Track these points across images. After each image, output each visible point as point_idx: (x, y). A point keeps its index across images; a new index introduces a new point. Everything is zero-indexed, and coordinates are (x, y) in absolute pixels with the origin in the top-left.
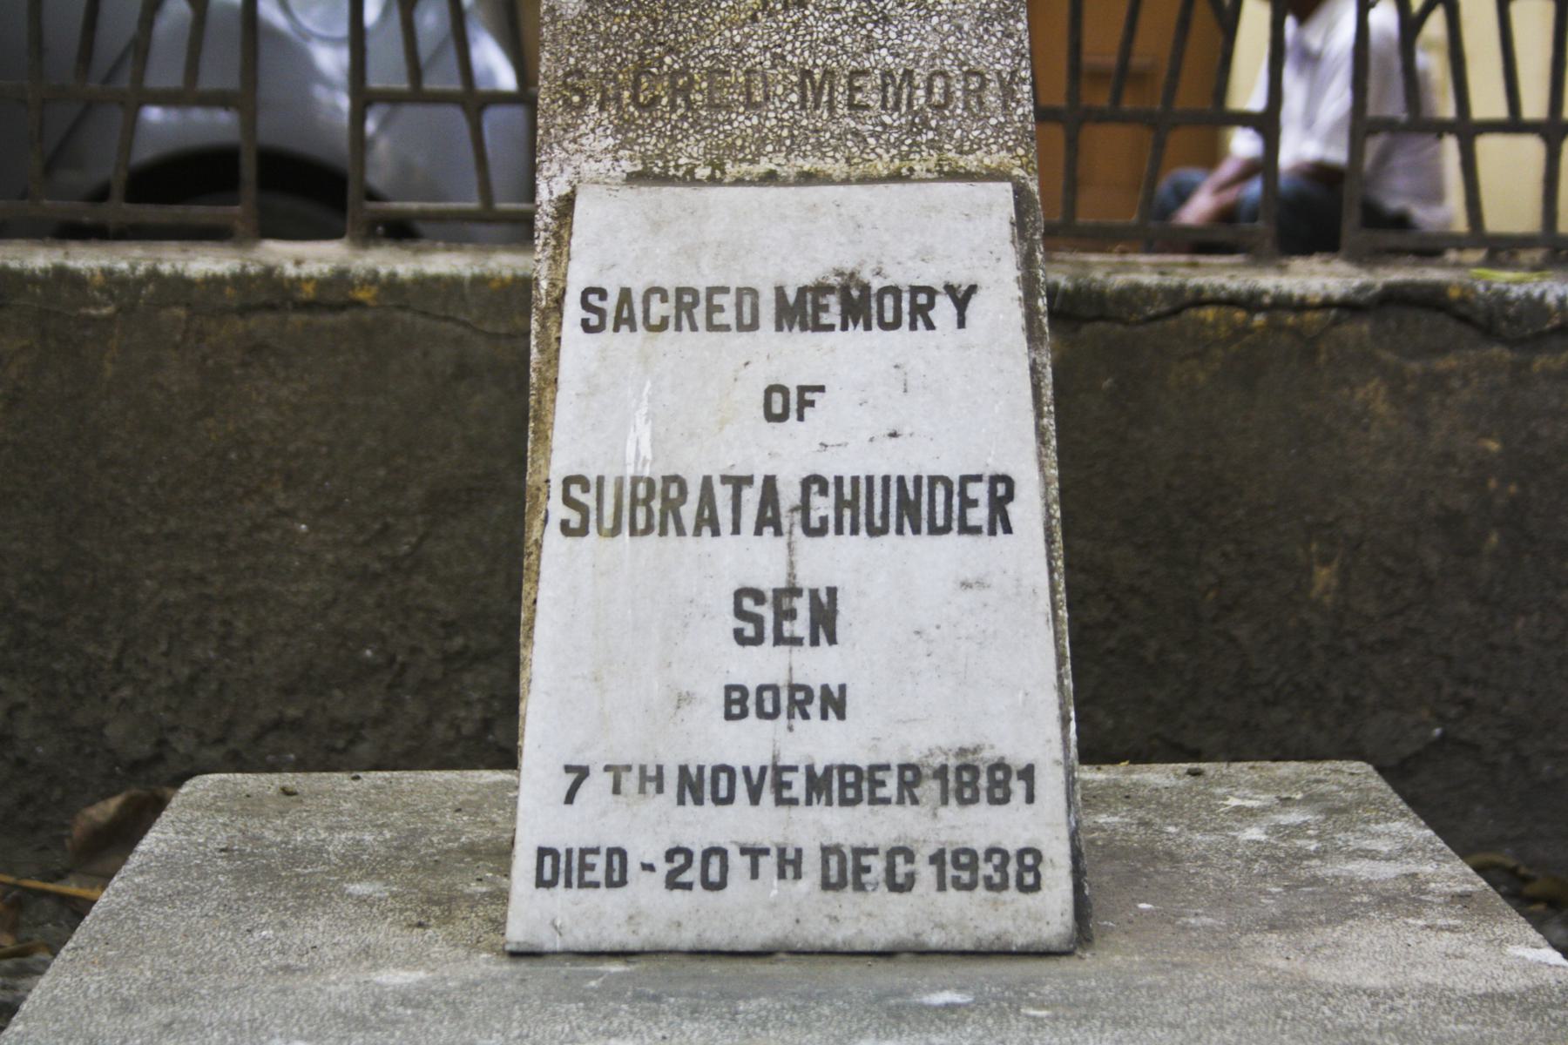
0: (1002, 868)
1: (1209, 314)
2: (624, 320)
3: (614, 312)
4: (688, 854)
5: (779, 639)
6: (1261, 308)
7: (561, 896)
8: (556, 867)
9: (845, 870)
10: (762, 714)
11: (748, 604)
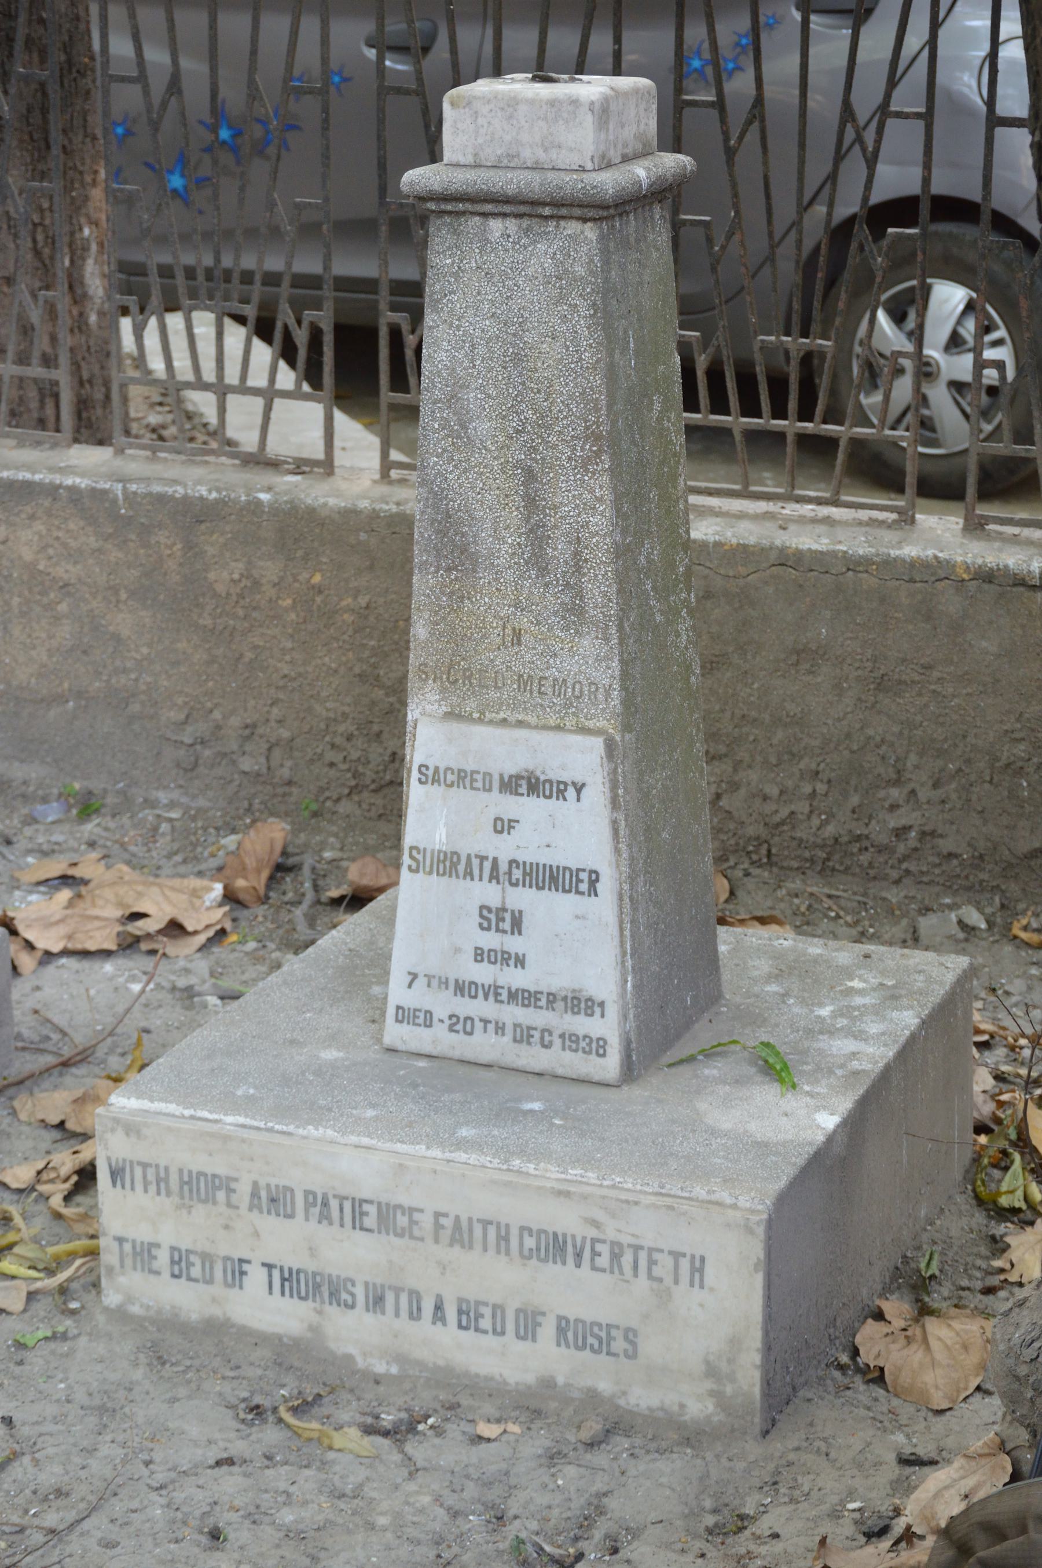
0: (590, 1044)
2: (435, 781)
3: (432, 776)
4: (458, 1018)
5: (498, 930)
7: (405, 1029)
8: (404, 1015)
9: (523, 1035)
10: (490, 962)
11: (485, 913)
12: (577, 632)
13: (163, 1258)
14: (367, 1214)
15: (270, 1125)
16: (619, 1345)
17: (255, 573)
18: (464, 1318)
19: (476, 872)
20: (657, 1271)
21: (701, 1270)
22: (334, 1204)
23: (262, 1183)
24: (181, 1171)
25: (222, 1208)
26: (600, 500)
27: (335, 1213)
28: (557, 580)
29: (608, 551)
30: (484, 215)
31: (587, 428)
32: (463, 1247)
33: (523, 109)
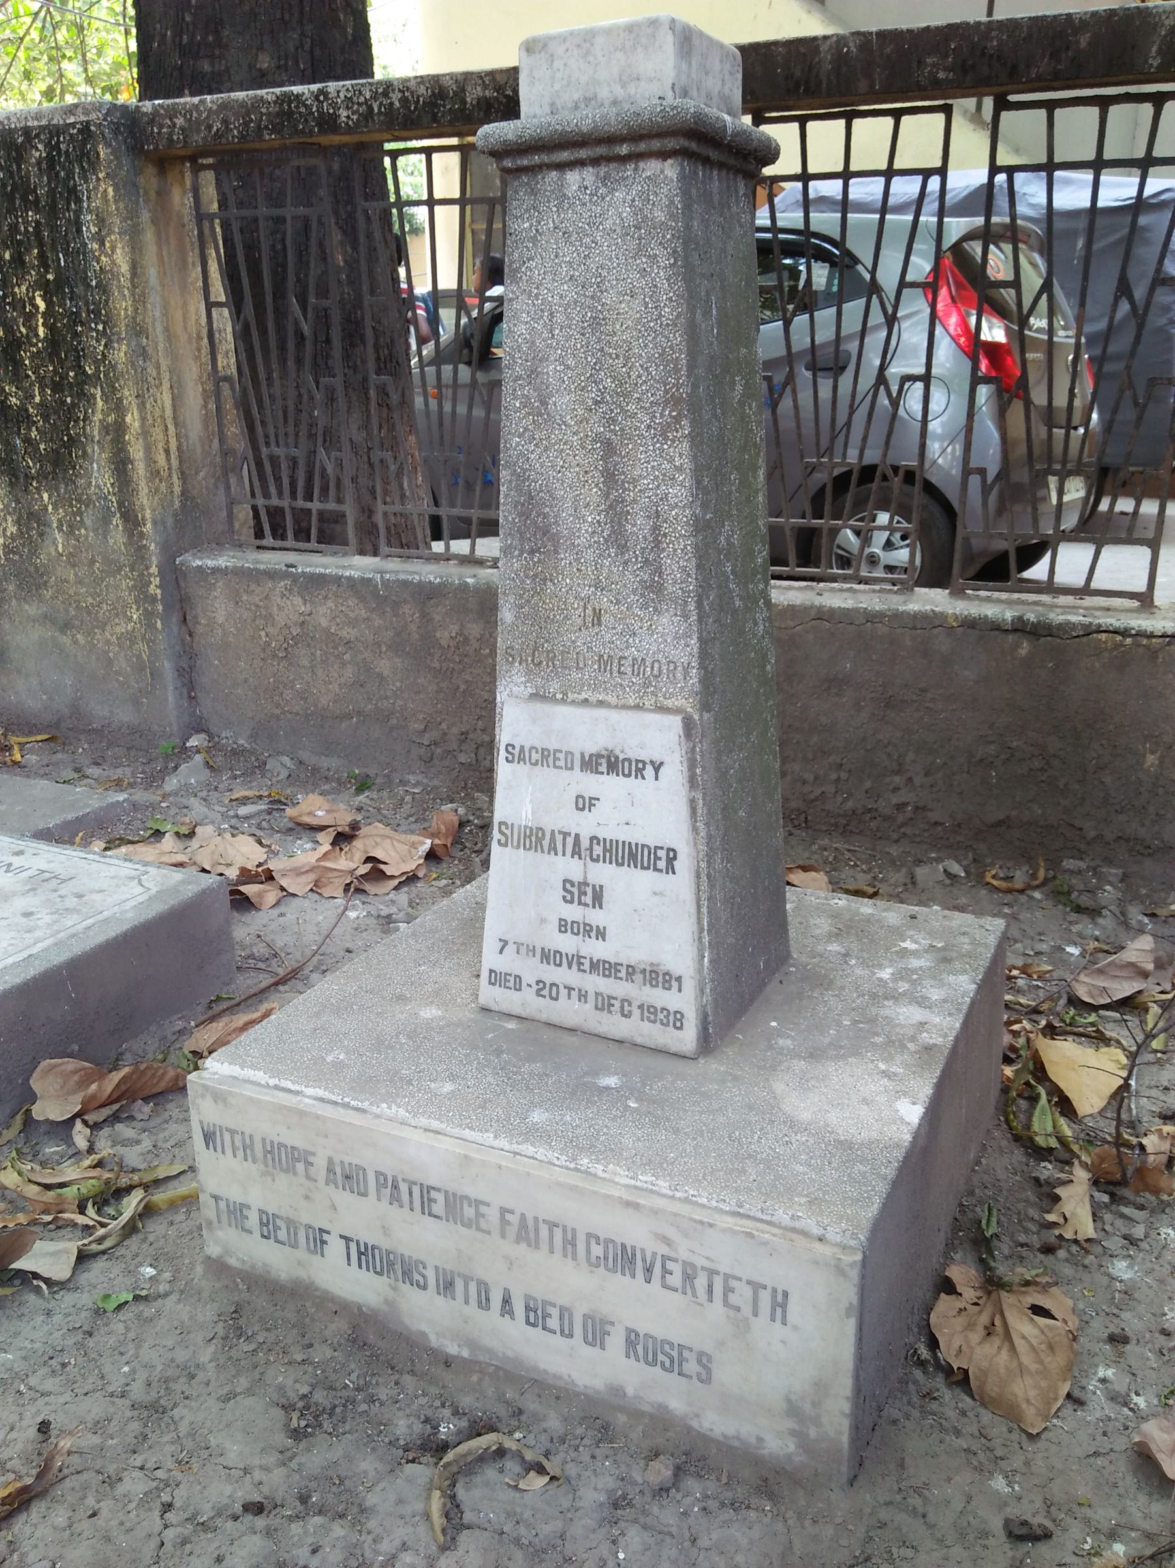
0: (667, 1017)
1: (1103, 636)
3: (519, 755)
5: (580, 903)
6: (1131, 636)
8: (497, 978)
9: (605, 1004)
11: (568, 886)
12: (656, 609)
13: (253, 1220)
14: (435, 1201)
15: (347, 1100)
16: (692, 1367)
17: (466, 632)
18: (532, 1314)
19: (560, 847)
20: (733, 1299)
21: (784, 1306)
22: (404, 1188)
23: (337, 1160)
24: (264, 1140)
25: (302, 1180)
26: (680, 469)
27: (405, 1197)
28: (636, 557)
29: (687, 523)
30: (561, 167)
31: (666, 392)
32: (529, 1245)
33: (600, 41)
